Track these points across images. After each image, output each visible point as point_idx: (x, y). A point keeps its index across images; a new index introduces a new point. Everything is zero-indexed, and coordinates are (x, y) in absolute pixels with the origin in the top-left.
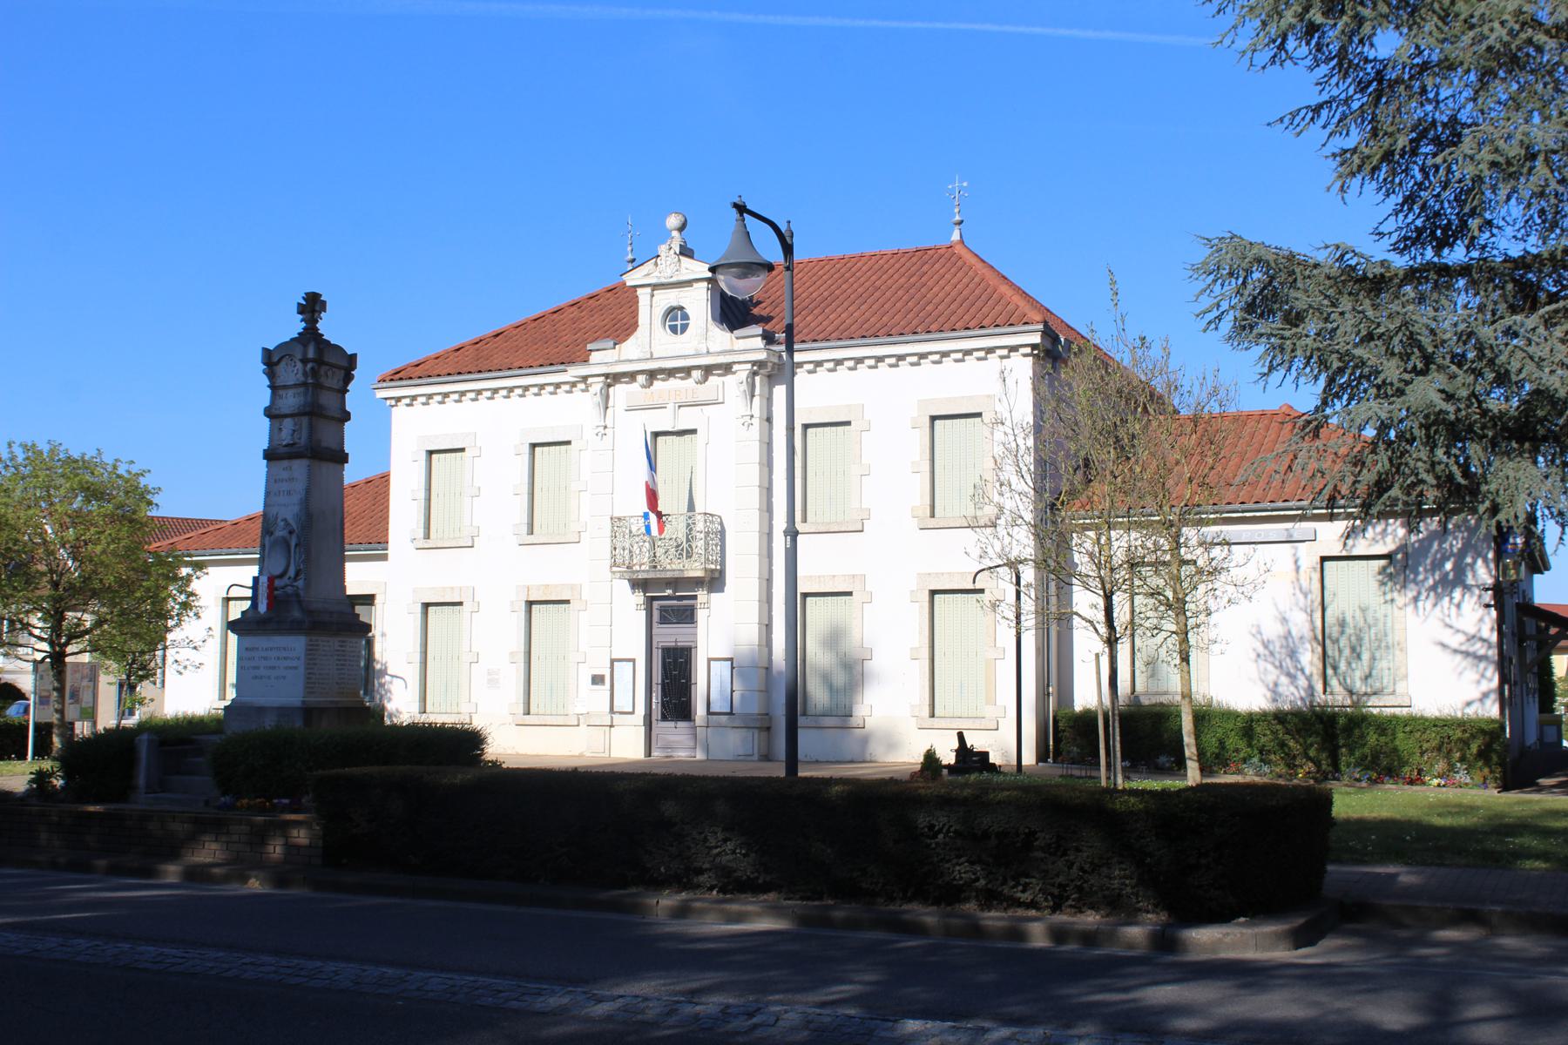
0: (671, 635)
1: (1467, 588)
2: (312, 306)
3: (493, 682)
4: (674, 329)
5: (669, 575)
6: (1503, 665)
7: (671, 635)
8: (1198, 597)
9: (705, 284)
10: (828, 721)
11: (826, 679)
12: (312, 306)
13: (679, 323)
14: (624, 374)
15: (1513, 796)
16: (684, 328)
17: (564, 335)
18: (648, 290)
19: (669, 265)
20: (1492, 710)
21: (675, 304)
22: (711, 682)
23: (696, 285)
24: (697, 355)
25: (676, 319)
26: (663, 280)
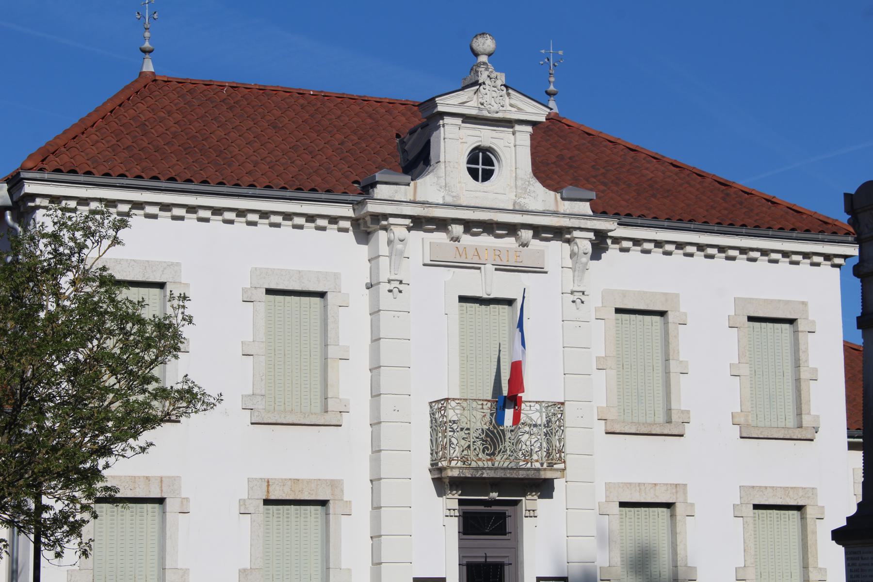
0: (488, 548)
4: (473, 173)
5: (522, 475)
7: (488, 548)
9: (529, 129)
13: (480, 167)
16: (487, 175)
18: (459, 121)
19: (492, 96)
21: (486, 143)
23: (518, 127)
25: (482, 164)
26: (485, 114)
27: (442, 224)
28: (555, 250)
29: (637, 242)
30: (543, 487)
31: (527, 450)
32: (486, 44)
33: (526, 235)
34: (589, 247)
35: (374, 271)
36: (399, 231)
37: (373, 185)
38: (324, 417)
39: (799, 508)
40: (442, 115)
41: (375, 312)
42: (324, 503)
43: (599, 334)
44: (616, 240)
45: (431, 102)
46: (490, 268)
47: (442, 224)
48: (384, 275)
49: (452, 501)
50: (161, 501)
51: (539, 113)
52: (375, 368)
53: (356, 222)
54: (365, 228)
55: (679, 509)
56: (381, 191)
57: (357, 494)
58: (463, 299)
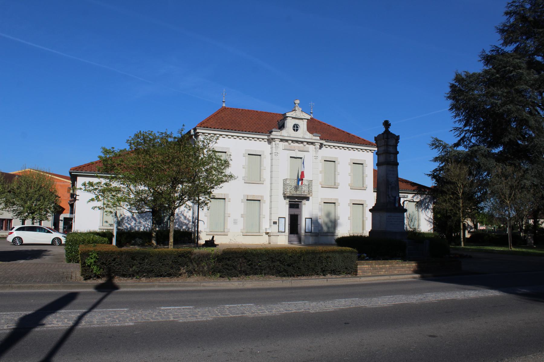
0: (295, 211)
1: (429, 209)
2: (387, 124)
3: (235, 222)
4: (294, 130)
6: (434, 224)
7: (295, 211)
8: (57, 194)
10: (329, 234)
11: (326, 224)
12: (387, 124)
14: (284, 140)
15: (340, 248)
16: (297, 130)
17: (266, 124)
20: (432, 231)
21: (297, 123)
22: (304, 225)
24: (309, 139)
25: (296, 128)
27: (287, 141)
28: (311, 147)
29: (329, 146)
30: (307, 199)
31: (303, 191)
32: (297, 102)
33: (305, 143)
34: (319, 147)
35: (272, 151)
36: (277, 142)
37: (272, 132)
38: (260, 182)
39: (362, 204)
40: (287, 117)
41: (272, 160)
42: (259, 200)
43: (320, 165)
44: (325, 145)
45: (285, 114)
46: (297, 150)
47: (287, 141)
48: (274, 152)
49: (287, 201)
50: (224, 199)
51: (309, 117)
52: (271, 172)
53: (268, 140)
54: (270, 141)
55: (336, 204)
56: (274, 133)
57: (267, 199)
58: (291, 157)
